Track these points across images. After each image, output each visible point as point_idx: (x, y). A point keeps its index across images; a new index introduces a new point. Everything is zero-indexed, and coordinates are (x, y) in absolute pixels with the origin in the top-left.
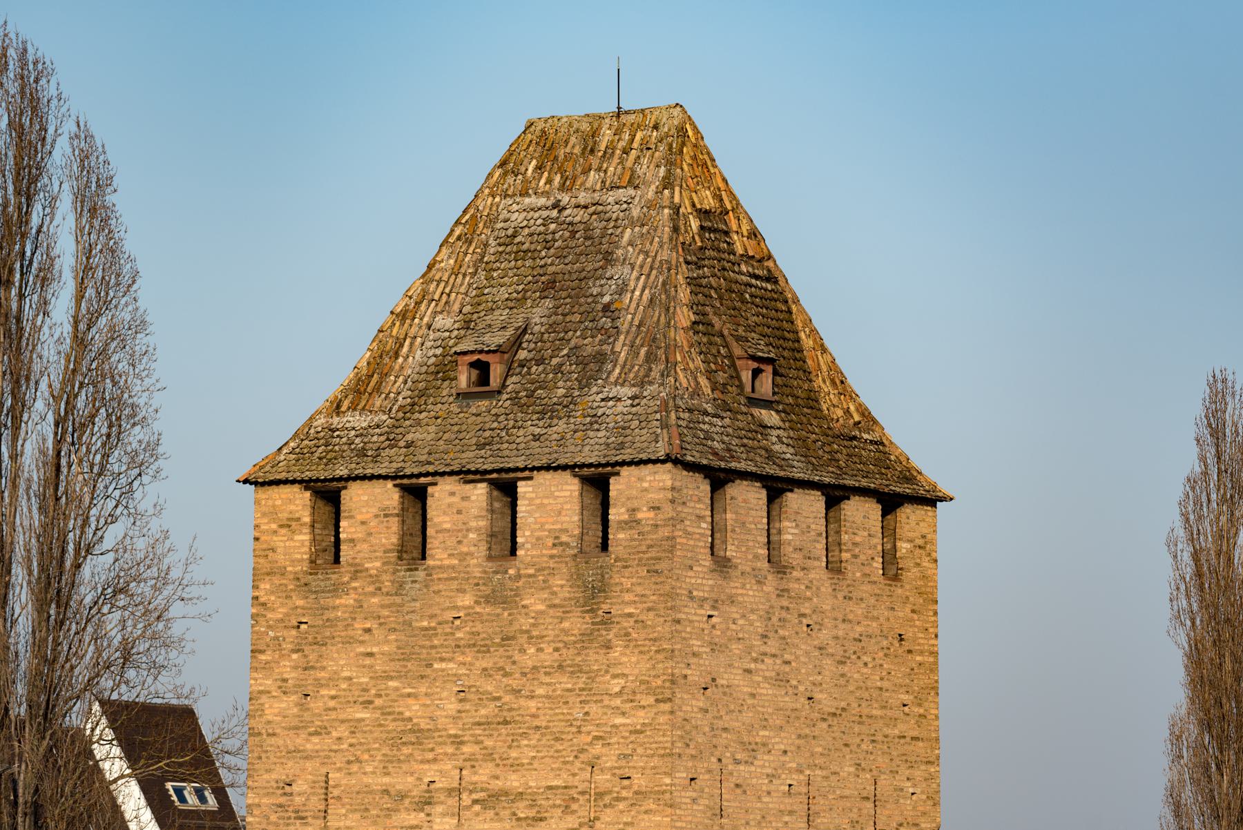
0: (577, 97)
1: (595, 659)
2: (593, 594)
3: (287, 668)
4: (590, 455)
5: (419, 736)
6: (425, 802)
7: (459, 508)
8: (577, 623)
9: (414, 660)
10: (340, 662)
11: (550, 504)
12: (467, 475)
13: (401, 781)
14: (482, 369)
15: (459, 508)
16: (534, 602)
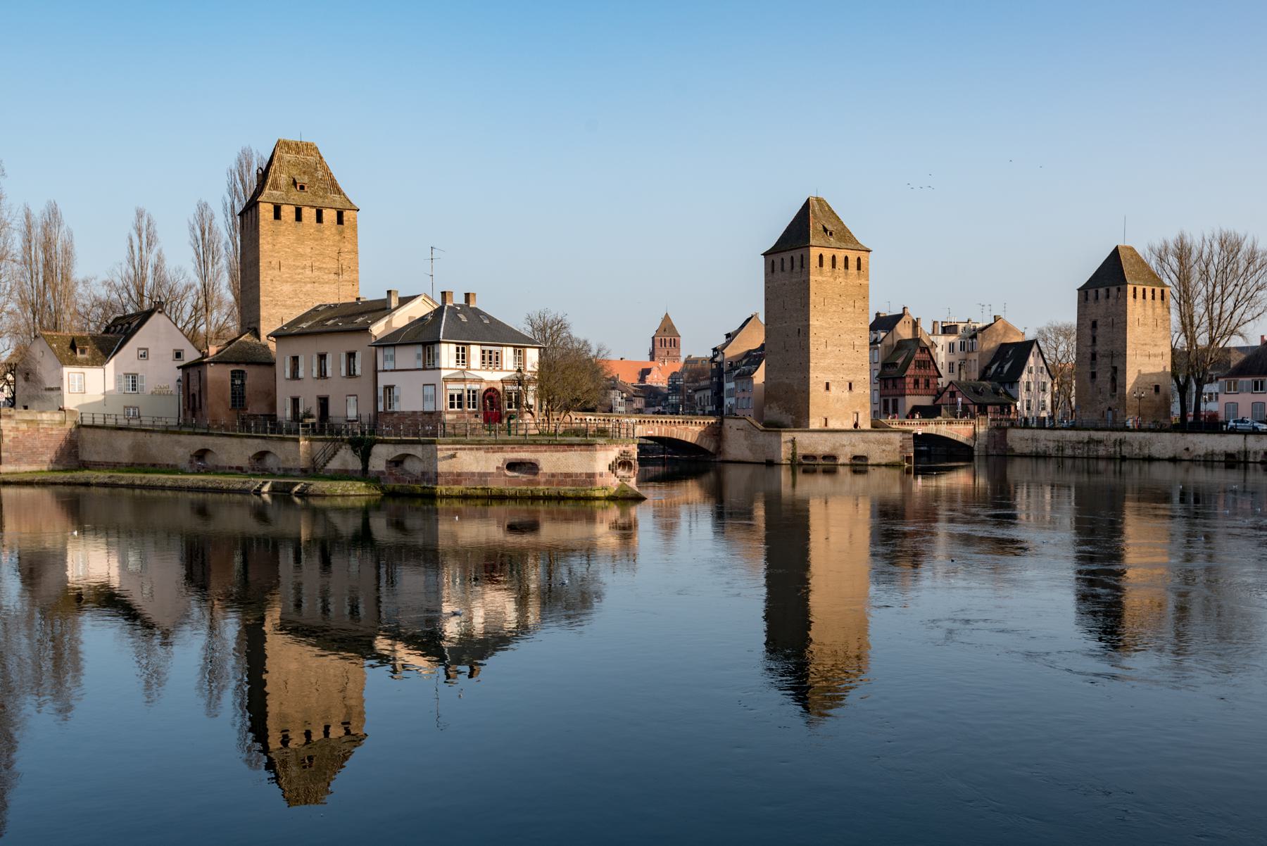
0: (292, 137)
1: (341, 245)
2: (341, 233)
3: (269, 239)
4: (339, 206)
5: (302, 255)
6: (304, 268)
7: (309, 214)
8: (337, 238)
9: (300, 240)
10: (282, 239)
11: (330, 215)
12: (312, 207)
13: (297, 264)
14: (302, 188)
15: (309, 214)
16: (328, 233)
